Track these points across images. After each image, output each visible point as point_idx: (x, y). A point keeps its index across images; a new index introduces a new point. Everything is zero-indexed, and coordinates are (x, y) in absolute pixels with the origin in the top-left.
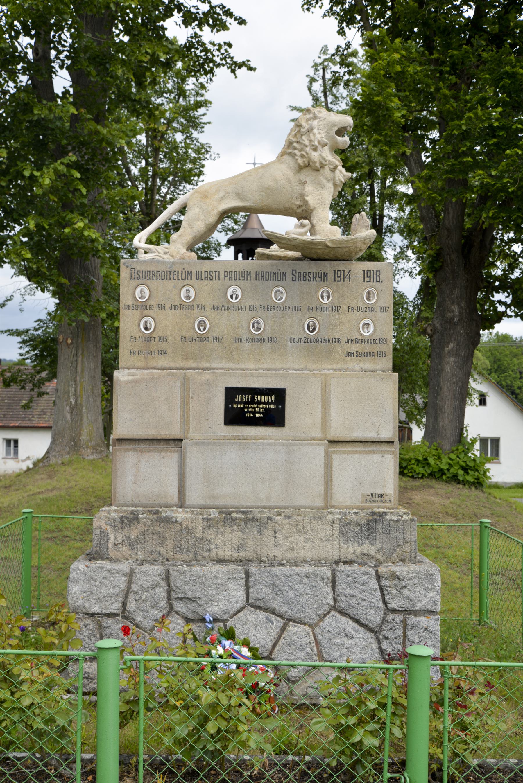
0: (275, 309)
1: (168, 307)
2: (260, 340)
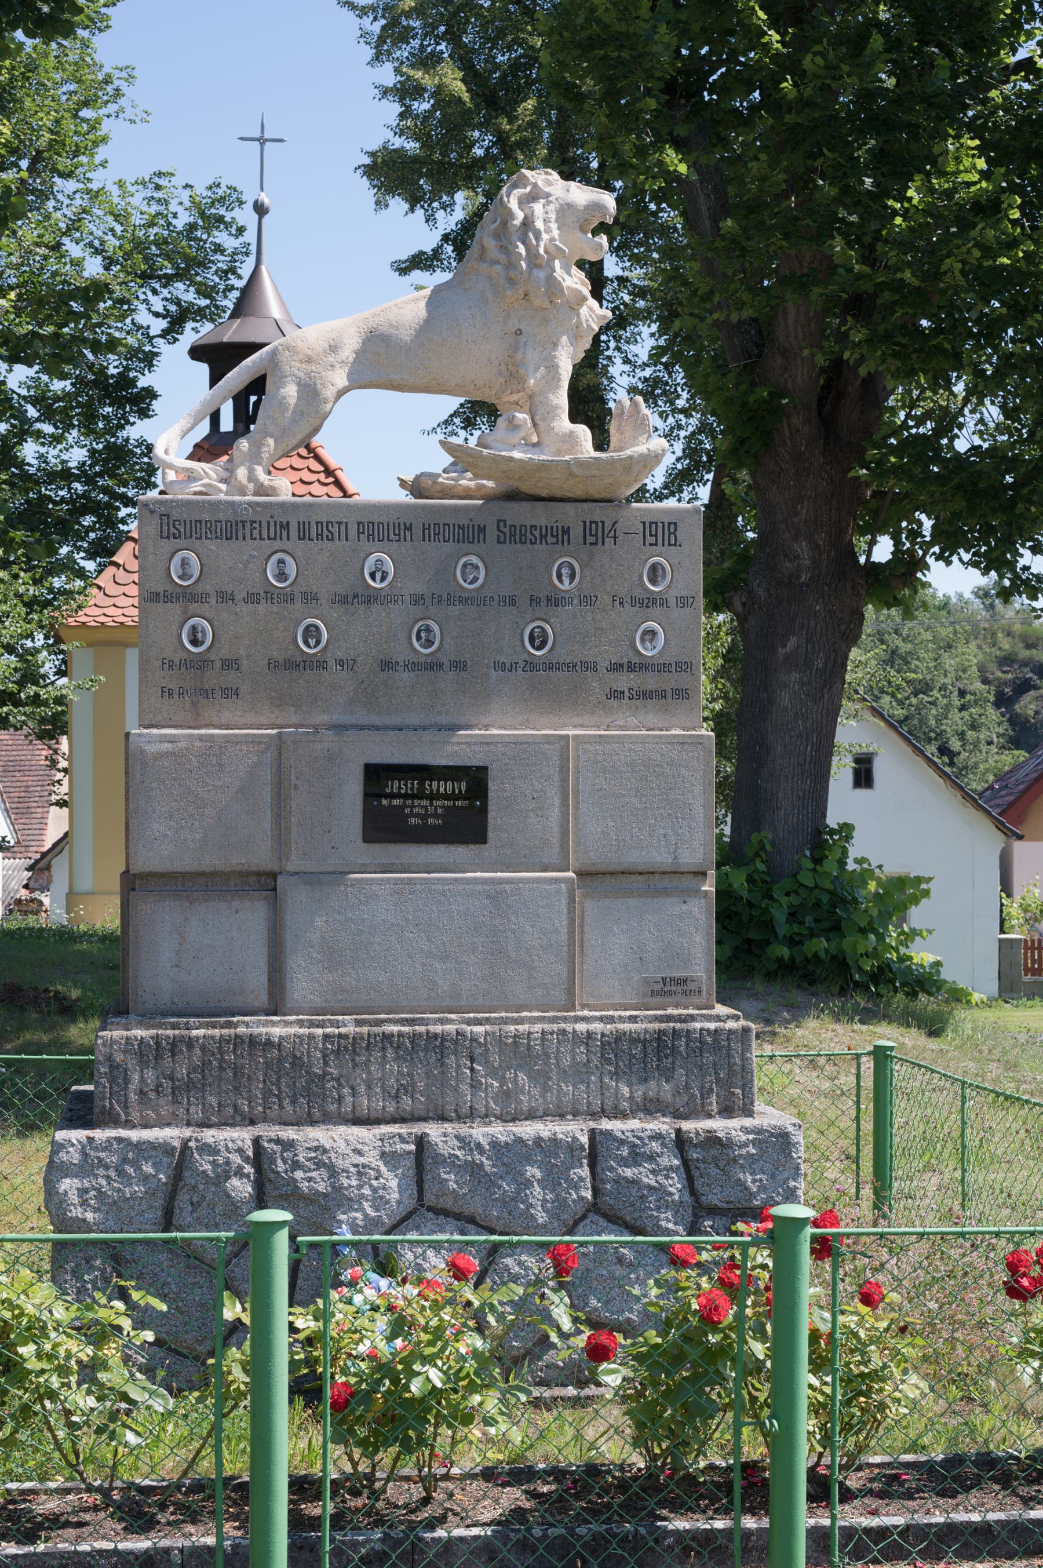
0: (463, 601)
1: (240, 595)
2: (433, 666)
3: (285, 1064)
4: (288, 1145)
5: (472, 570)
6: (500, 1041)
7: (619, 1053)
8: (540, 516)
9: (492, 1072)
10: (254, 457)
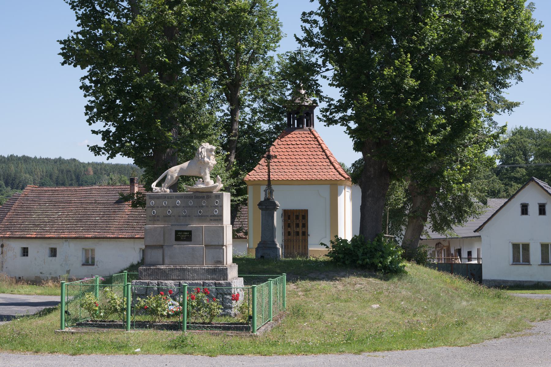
2: (185, 216)
3: (163, 272)
4: (162, 283)
5: (191, 203)
6: (192, 269)
7: (208, 271)
8: (201, 195)
9: (191, 274)
10: (164, 186)
